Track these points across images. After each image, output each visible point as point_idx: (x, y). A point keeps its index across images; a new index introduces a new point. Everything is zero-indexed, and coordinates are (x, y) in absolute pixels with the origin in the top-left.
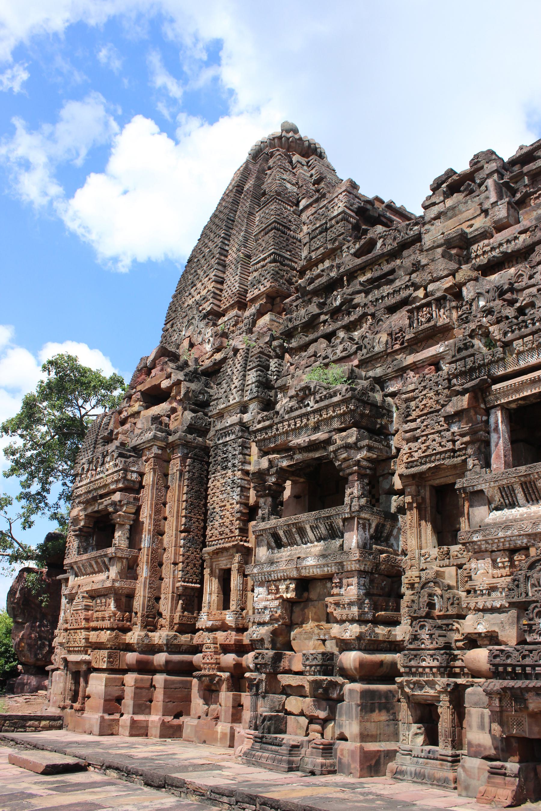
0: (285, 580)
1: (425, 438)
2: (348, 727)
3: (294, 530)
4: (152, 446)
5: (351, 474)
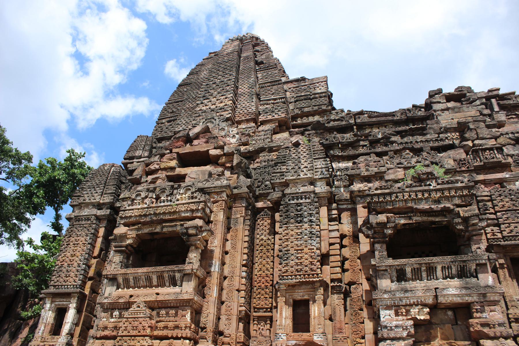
3: (423, 268)
4: (222, 192)
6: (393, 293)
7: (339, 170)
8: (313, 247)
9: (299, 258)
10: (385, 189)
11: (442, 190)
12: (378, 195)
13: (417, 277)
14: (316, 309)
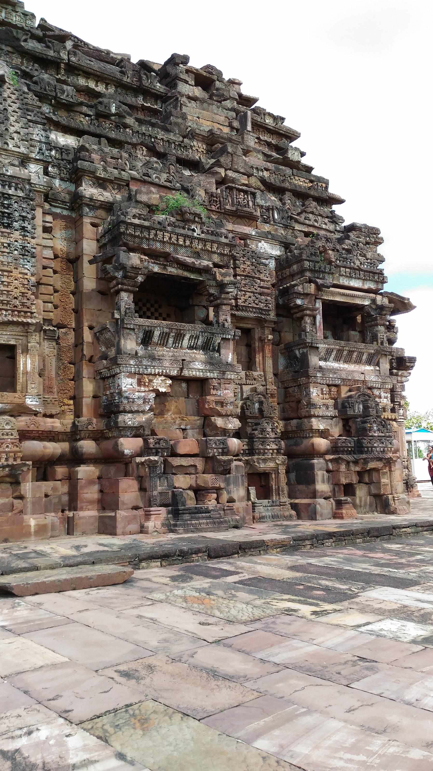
0: (160, 376)
1: (244, 293)
2: (235, 492)
5: (225, 305)
6: (140, 359)
7: (55, 148)
8: (26, 271)
9: (5, 283)
10: (144, 220)
11: (204, 241)
12: (136, 226)
13: (162, 342)
14: (29, 362)
